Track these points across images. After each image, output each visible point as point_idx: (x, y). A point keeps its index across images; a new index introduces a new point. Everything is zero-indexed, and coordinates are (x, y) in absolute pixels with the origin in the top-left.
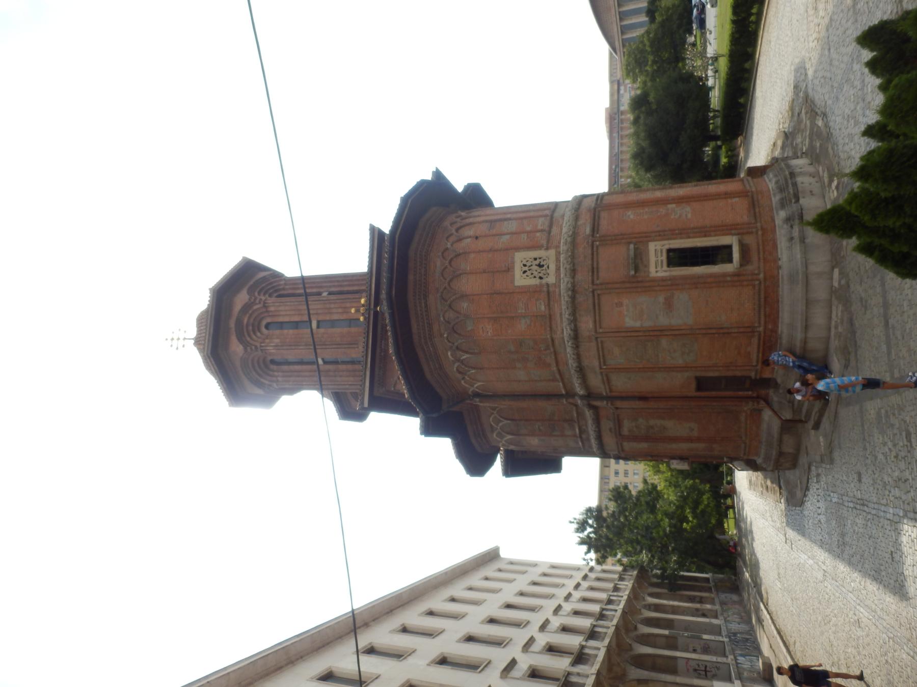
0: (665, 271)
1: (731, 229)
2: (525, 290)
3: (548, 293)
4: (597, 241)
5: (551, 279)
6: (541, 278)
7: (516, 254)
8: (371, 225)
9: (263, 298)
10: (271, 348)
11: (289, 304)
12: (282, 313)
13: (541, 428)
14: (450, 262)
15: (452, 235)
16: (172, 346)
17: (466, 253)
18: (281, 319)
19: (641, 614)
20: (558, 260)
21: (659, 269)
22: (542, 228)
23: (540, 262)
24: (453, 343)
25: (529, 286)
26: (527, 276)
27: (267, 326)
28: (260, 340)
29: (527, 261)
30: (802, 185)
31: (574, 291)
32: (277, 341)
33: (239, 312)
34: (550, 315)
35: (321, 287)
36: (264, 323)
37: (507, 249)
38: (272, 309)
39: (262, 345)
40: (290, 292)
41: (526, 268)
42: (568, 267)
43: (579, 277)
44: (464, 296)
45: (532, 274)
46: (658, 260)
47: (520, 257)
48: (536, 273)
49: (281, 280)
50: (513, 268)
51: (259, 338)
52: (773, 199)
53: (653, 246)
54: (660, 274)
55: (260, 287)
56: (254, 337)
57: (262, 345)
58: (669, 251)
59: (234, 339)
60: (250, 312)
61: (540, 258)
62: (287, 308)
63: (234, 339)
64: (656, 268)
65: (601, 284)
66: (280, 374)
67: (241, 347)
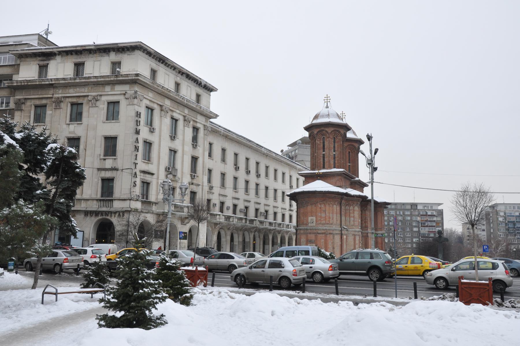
2: (308, 219)
3: (307, 224)
5: (309, 225)
16: (325, 98)
19: (286, 234)
20: (313, 226)
31: (307, 229)
32: (319, 143)
35: (337, 151)
36: (325, 137)
40: (336, 141)
43: (309, 230)
47: (314, 218)
59: (318, 130)
63: (318, 130)
67: (316, 133)
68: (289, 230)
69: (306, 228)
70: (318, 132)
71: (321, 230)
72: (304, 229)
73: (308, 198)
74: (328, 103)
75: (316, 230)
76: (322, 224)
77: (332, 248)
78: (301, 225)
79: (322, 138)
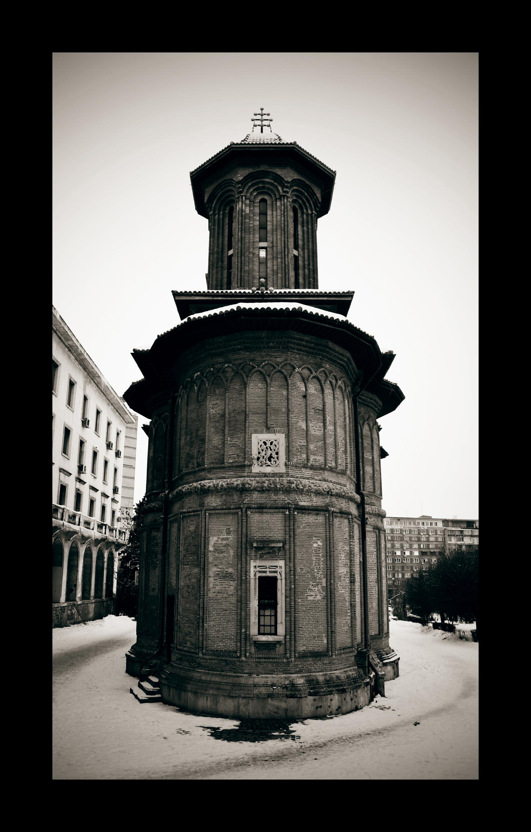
0: (255, 575)
1: (290, 636)
4: (289, 513)
5: (256, 469)
6: (258, 459)
7: (284, 435)
8: (354, 292)
9: (289, 195)
10: (240, 206)
11: (283, 218)
12: (274, 212)
13: (160, 459)
14: (280, 371)
15: (311, 373)
16: (255, 115)
17: (287, 387)
18: (269, 212)
20: (274, 475)
21: (258, 569)
22: (312, 460)
23: (274, 458)
24: (206, 377)
25: (251, 448)
26: (261, 446)
27: (263, 201)
28: (249, 195)
29: (276, 446)
30: (329, 700)
31: (243, 490)
32: (247, 211)
33: (275, 173)
34: (224, 468)
35: (303, 249)
36: (266, 197)
37: (288, 426)
38: (278, 204)
39: (244, 197)
40: (300, 219)
41: (268, 444)
42: (266, 485)
43: (255, 495)
44: (245, 385)
45: (263, 450)
46: (266, 568)
47: (280, 438)
48: (263, 454)
49: (312, 210)
50: (269, 433)
51: (251, 194)
52: (321, 673)
53: (281, 563)
54: (252, 570)
55: (303, 191)
56: (252, 190)
57: (244, 197)
58: (275, 579)
59: (251, 170)
60: (276, 184)
61: (278, 458)
62: (279, 217)
64: (259, 567)
65: (247, 516)
66: (221, 216)
68: (75, 528)
69: (237, 482)
70: (247, 179)
71: (309, 492)
72: (229, 490)
73: (246, 349)
74: (264, 128)
75: (288, 491)
76: (312, 468)
77: (347, 580)
78: (210, 470)
79: (258, 200)
